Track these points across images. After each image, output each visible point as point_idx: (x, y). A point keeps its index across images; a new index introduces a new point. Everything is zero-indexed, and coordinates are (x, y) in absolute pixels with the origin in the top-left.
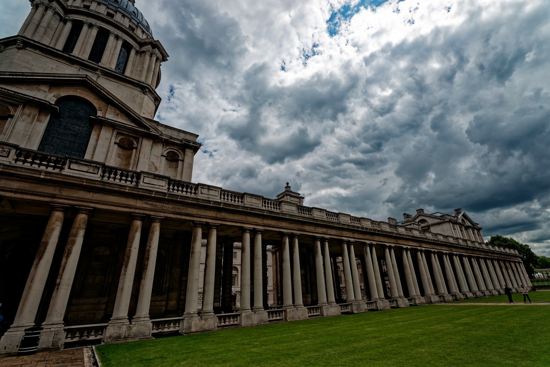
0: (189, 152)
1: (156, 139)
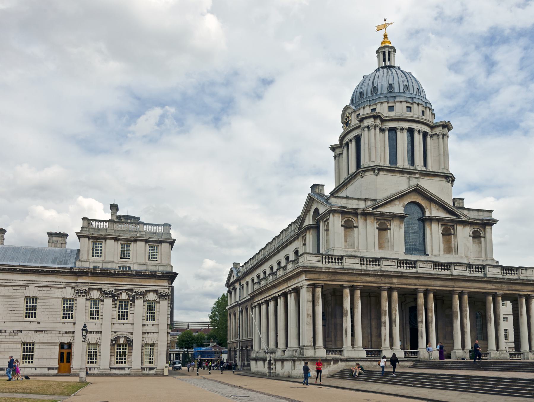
0: (488, 228)
1: (464, 223)
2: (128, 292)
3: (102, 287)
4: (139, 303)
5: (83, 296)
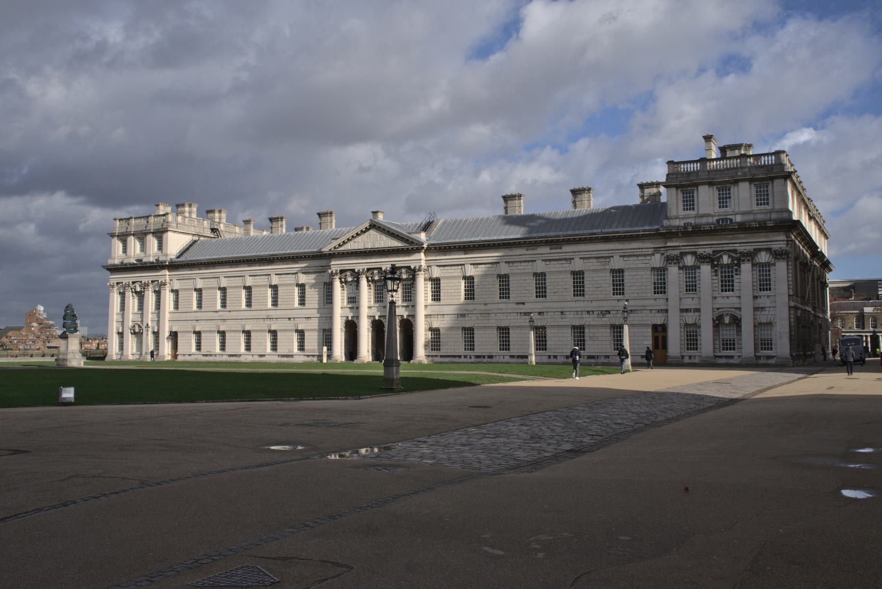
2: (731, 254)
3: (697, 250)
4: (746, 267)
5: (674, 263)
